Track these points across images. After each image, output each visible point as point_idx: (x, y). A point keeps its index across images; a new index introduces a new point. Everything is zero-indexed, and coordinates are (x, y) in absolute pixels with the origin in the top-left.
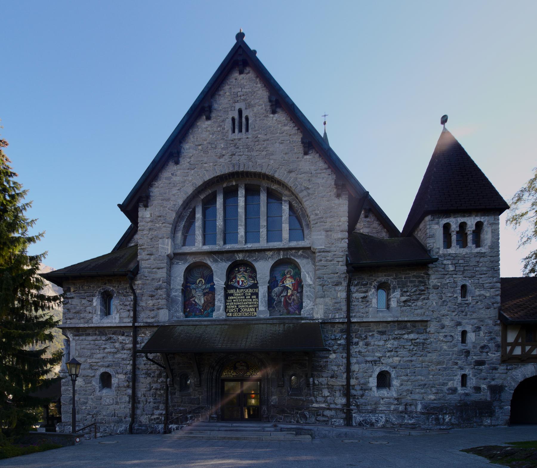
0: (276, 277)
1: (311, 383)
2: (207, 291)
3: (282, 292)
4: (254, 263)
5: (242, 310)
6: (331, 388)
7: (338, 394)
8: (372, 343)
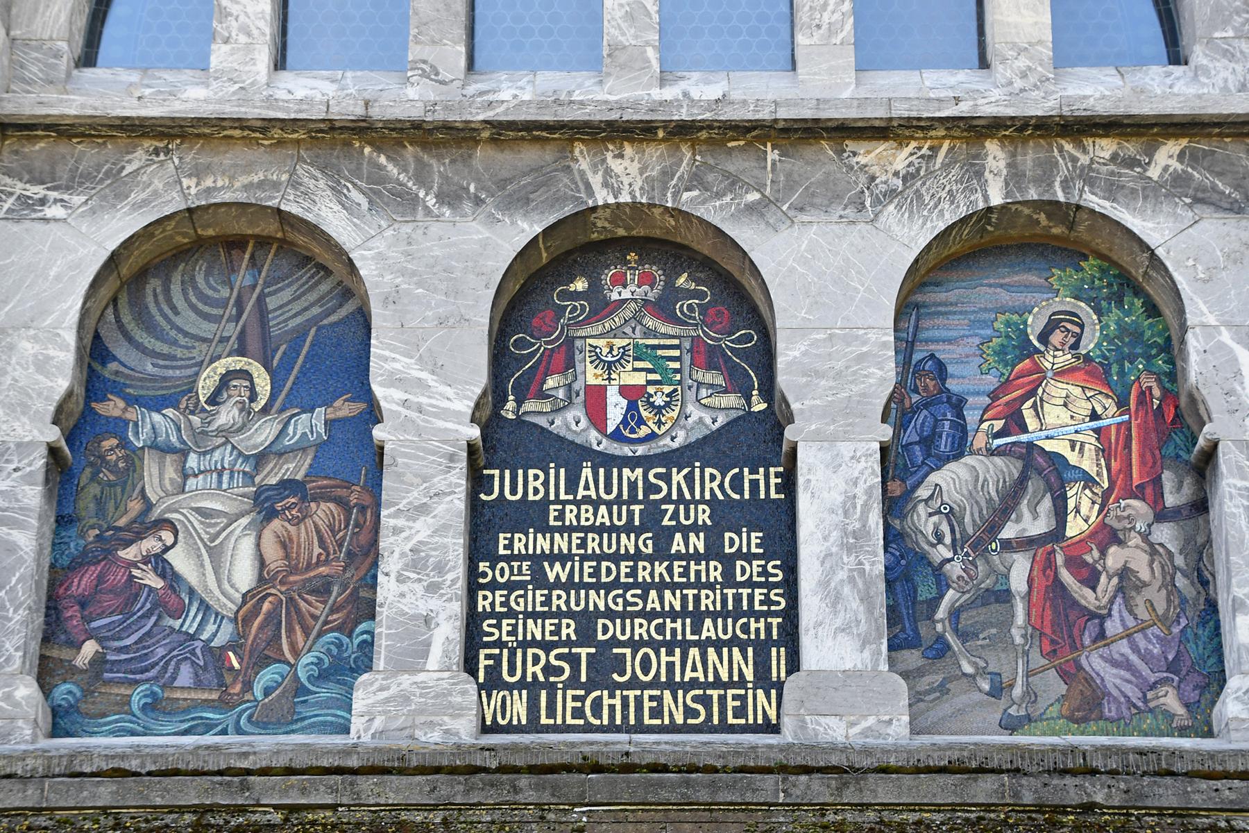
0: (941, 370)
2: (294, 468)
3: (1006, 507)
4: (744, 234)
5: (633, 665)
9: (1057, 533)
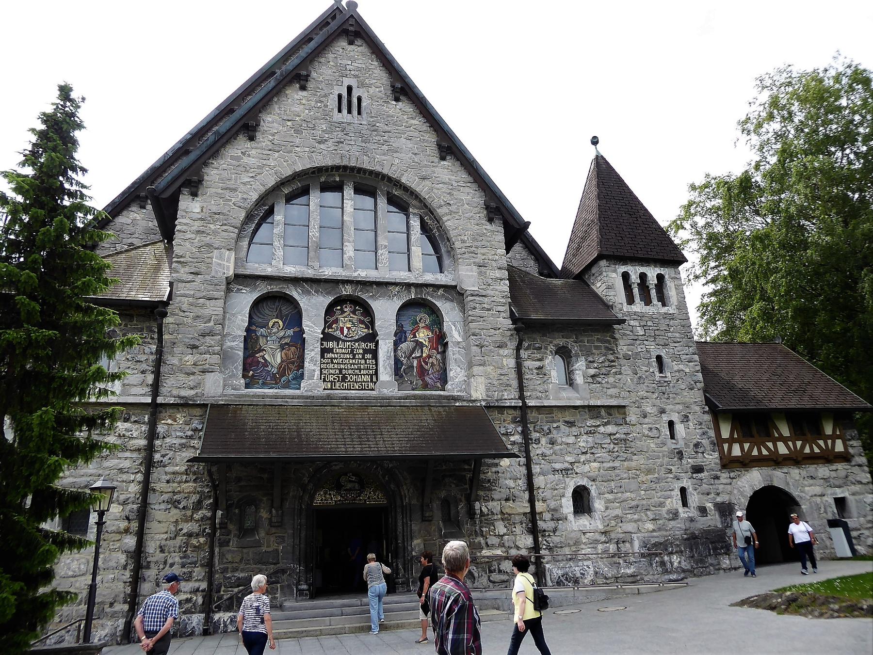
1: (478, 512)
2: (287, 340)
3: (413, 352)
6: (506, 518)
7: (518, 529)
8: (559, 440)
9: (421, 356)
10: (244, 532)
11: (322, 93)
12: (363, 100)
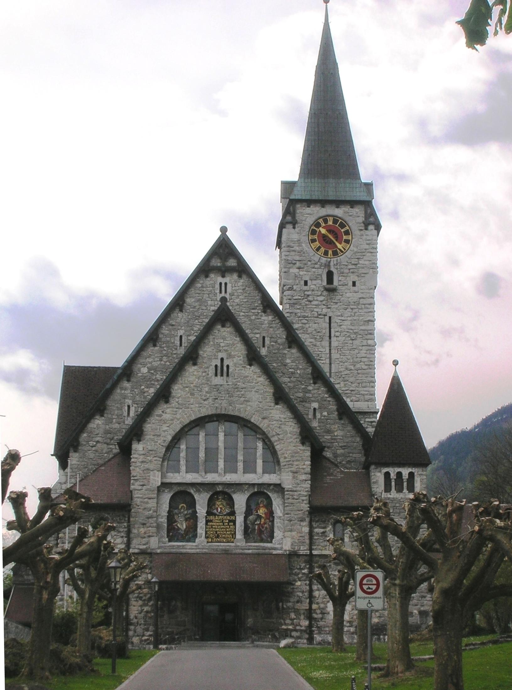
7: (302, 617)
10: (171, 612)
11: (206, 365)
12: (230, 367)
